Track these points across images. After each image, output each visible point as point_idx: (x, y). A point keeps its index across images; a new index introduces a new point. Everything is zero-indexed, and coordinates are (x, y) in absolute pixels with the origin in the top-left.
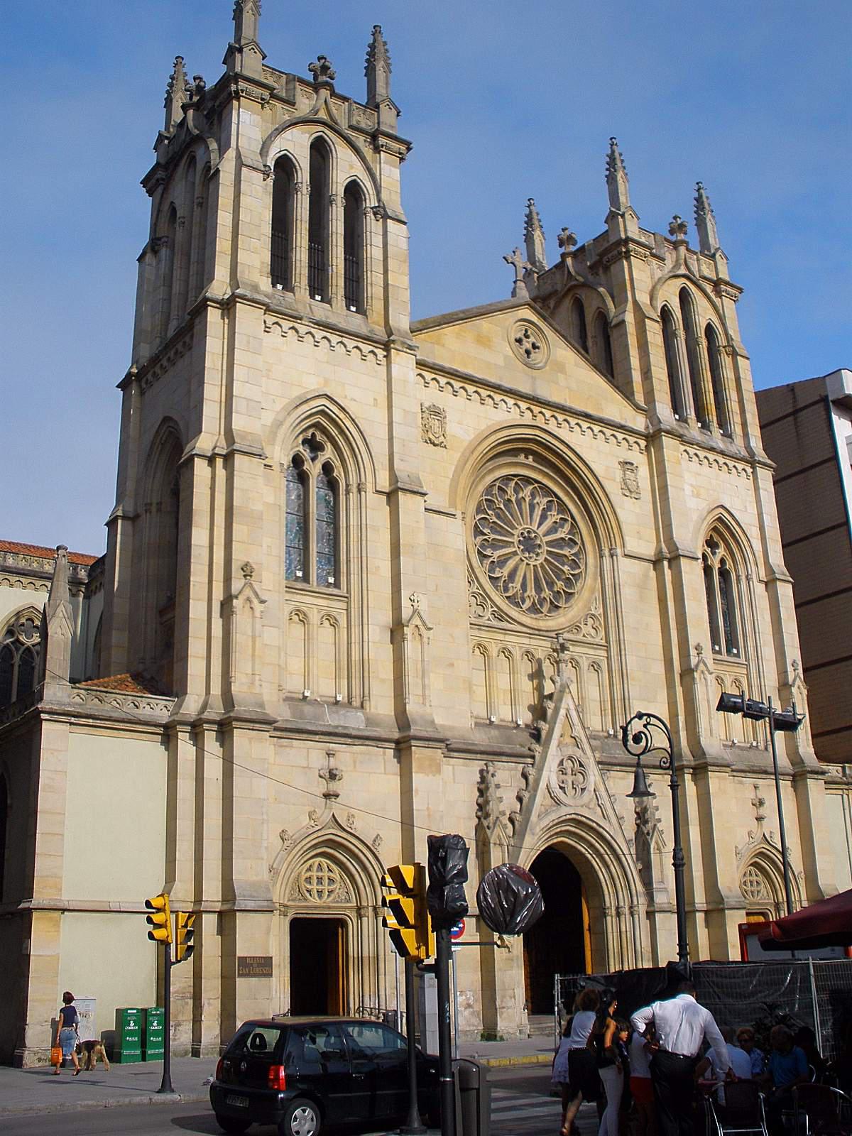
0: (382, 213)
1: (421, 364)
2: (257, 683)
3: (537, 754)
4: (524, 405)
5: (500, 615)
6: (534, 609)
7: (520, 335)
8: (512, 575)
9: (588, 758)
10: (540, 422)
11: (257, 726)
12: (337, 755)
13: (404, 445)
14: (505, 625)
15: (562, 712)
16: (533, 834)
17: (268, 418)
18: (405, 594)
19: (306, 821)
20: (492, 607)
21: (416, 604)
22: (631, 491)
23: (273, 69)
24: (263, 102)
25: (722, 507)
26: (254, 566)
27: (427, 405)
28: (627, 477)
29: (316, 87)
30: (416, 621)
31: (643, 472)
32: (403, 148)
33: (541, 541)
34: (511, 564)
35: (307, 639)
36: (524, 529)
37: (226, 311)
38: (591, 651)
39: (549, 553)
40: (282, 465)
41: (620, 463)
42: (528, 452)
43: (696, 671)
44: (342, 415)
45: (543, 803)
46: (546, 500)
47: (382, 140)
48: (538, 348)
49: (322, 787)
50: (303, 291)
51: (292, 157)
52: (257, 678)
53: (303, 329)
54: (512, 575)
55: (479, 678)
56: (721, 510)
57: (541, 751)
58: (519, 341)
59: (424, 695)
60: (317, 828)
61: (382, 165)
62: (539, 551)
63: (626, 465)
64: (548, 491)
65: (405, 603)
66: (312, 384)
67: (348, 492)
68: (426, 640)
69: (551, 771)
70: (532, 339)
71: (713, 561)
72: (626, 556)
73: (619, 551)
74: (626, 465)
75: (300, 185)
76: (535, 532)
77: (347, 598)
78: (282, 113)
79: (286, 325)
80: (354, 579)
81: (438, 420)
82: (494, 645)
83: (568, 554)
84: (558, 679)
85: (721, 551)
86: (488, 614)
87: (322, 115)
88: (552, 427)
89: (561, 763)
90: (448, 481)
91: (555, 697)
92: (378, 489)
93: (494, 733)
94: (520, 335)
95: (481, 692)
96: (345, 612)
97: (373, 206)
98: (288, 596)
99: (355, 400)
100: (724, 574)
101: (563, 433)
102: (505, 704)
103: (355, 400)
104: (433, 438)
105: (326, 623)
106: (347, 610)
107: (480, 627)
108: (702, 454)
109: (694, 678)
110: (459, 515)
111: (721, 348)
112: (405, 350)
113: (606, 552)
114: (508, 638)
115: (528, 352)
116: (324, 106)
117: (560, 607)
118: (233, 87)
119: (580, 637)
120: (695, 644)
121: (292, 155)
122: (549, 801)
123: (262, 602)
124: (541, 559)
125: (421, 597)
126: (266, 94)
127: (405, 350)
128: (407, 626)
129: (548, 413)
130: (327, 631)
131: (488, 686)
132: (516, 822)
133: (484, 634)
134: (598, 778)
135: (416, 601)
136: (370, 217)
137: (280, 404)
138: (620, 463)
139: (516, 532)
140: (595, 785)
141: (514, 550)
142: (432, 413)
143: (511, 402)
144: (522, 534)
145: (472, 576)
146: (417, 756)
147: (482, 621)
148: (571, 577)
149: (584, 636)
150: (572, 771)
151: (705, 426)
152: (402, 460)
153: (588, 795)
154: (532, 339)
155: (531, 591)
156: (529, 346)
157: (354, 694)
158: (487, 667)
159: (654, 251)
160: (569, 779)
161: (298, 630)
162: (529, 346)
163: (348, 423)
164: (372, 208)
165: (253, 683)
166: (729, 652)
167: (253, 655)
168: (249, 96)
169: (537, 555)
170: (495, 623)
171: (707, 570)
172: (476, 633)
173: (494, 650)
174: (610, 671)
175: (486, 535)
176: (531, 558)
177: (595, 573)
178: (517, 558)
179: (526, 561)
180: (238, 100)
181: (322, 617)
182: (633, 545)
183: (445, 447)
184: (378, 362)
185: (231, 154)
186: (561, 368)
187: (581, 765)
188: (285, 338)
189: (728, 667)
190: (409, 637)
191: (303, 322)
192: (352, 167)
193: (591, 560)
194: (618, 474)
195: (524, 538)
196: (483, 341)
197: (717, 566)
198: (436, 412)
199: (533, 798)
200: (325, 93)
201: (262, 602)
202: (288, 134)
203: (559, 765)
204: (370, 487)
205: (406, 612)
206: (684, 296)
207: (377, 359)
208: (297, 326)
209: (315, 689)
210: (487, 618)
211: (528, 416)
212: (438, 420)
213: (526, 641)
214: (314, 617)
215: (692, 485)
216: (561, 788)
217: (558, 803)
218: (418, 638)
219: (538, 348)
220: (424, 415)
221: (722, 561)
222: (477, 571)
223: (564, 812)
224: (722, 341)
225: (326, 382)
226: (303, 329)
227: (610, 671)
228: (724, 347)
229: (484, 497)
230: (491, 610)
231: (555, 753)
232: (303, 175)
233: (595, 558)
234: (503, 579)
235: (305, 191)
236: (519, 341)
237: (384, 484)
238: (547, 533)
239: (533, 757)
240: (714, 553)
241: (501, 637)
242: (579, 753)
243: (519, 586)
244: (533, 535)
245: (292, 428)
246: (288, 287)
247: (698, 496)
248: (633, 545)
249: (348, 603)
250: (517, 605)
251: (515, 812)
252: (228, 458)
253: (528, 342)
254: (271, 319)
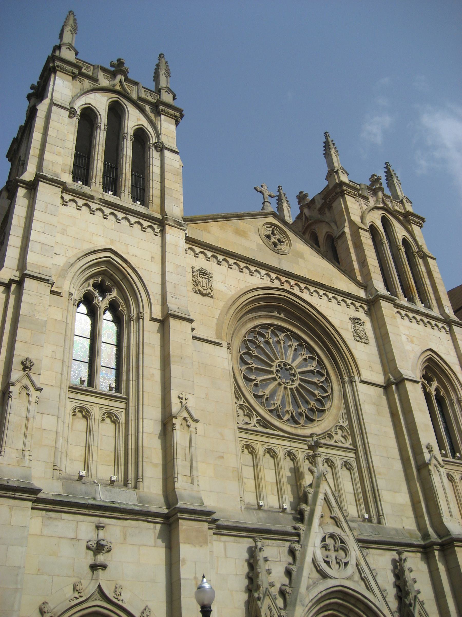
0: (161, 148)
1: (188, 240)
2: (27, 458)
3: (301, 532)
4: (273, 276)
5: (265, 423)
6: (294, 420)
7: (269, 232)
8: (273, 393)
9: (348, 536)
10: (286, 287)
11: (19, 495)
12: (107, 528)
13: (175, 288)
15: (321, 496)
16: (303, 605)
17: (61, 261)
18: (174, 394)
19: (69, 593)
20: (257, 417)
21: (184, 401)
22: (361, 338)
23: (84, 62)
24: (74, 77)
25: (431, 350)
26: (33, 361)
27: (197, 268)
28: (357, 328)
29: (113, 75)
30: (185, 414)
31: (368, 326)
32: (177, 114)
33: (295, 371)
35: (89, 431)
36: (281, 362)
37: (33, 190)
38: (343, 453)
39: (301, 380)
40: (71, 294)
41: (350, 319)
42: (280, 310)
43: (430, 464)
44: (124, 265)
45: (310, 576)
46: (296, 344)
47: (161, 107)
48: (283, 242)
49: (89, 558)
50: (97, 185)
51: (94, 108)
52: (27, 453)
53: (94, 206)
54: (273, 393)
55: (248, 472)
56: (430, 353)
57: (304, 529)
58: (268, 237)
59: (192, 476)
60: (81, 600)
61: (162, 122)
62: (294, 379)
63: (355, 320)
64: (298, 338)
65: (175, 400)
67: (129, 321)
68: (193, 430)
69: (315, 546)
70: (277, 236)
71: (430, 390)
72: (363, 382)
73: (357, 378)
74: (355, 320)
75: (99, 124)
76: (289, 365)
77: (126, 400)
78: (87, 84)
79: (81, 202)
80: (132, 384)
81: (206, 278)
82: (260, 446)
83: (317, 382)
84: (315, 469)
85: (435, 384)
86: (254, 421)
87: (118, 88)
88: (296, 291)
89: (324, 540)
90: (215, 320)
91: (314, 485)
92: (154, 316)
93: (261, 514)
94: (269, 232)
95: (250, 484)
96: (124, 410)
97: (154, 142)
98: (72, 395)
99: (136, 256)
100: (440, 401)
101: (305, 296)
102: (273, 494)
103: (136, 256)
104: (202, 289)
105: (108, 420)
106: (126, 409)
107: (247, 431)
108: (411, 315)
109: (429, 471)
110: (224, 344)
111: (415, 253)
112: (176, 226)
113: (347, 379)
114: (272, 441)
115: (275, 245)
116: (119, 84)
117: (315, 420)
118: (51, 65)
119: (332, 443)
120: (426, 444)
121: (95, 107)
122: (316, 575)
123: (40, 390)
124: (296, 384)
125: (188, 396)
126: (76, 71)
127: (176, 226)
128: (176, 418)
129: (293, 282)
130: (109, 426)
131: (257, 479)
132: (287, 595)
133: (251, 437)
134: (358, 553)
135: (184, 399)
136: (153, 150)
137: (73, 253)
138: (350, 319)
139: (274, 364)
140: (357, 560)
141: (273, 376)
142: (200, 273)
143: (263, 272)
144: (279, 366)
145: (239, 393)
146: (184, 527)
148: (321, 398)
149: (336, 442)
150: (334, 547)
151: (411, 300)
152: (174, 297)
153: (351, 569)
154: (277, 236)
155: (290, 407)
156: (276, 240)
157: (129, 477)
158: (255, 465)
159: (360, 192)
160: (333, 554)
161: (81, 424)
162: (276, 240)
163: (130, 271)
164: (154, 144)
165: (22, 457)
166: (454, 456)
167: (26, 433)
168: (63, 71)
169: (293, 381)
171: (427, 396)
172: (244, 435)
173: (260, 450)
174: (360, 469)
175: (250, 364)
176: (288, 383)
177: (340, 396)
178: (276, 383)
179: (283, 385)
180: (55, 73)
181: (104, 414)
182: (366, 375)
183: (212, 297)
184: (155, 233)
185: (46, 102)
186: (300, 255)
187: (342, 542)
188: (80, 211)
189: (455, 467)
190: (178, 426)
191: (95, 201)
192: (139, 120)
193: (336, 387)
194: (350, 326)
195: (281, 369)
197: (434, 393)
198: (203, 273)
199: (301, 569)
200: (120, 77)
201: (40, 390)
203: (322, 542)
204: (146, 316)
205: (175, 407)
206: (384, 220)
207: (154, 232)
208: (90, 203)
209: (94, 472)
210: (253, 424)
212: (206, 278)
213: (287, 443)
214: (96, 413)
215: (406, 335)
216: (325, 561)
217: (324, 576)
218: (186, 428)
219: (283, 242)
220: (194, 274)
221: (437, 390)
222: (243, 389)
223: (330, 583)
224: (415, 249)
226: (94, 206)
227: (360, 469)
228: (416, 253)
229: (247, 338)
230: (256, 419)
231: (317, 531)
232: (103, 119)
233: (339, 385)
234: (266, 397)
235: (102, 128)
236: (268, 237)
237: (157, 313)
238: (299, 366)
239: (298, 535)
240: (431, 385)
241: (266, 440)
242: (337, 531)
243: (279, 403)
244: (288, 367)
245: (81, 270)
246: (87, 182)
247: (412, 342)
248: (366, 375)
249: (126, 404)
250: (279, 417)
251: (284, 585)
252: (20, 283)
253: (275, 238)
254: (67, 197)
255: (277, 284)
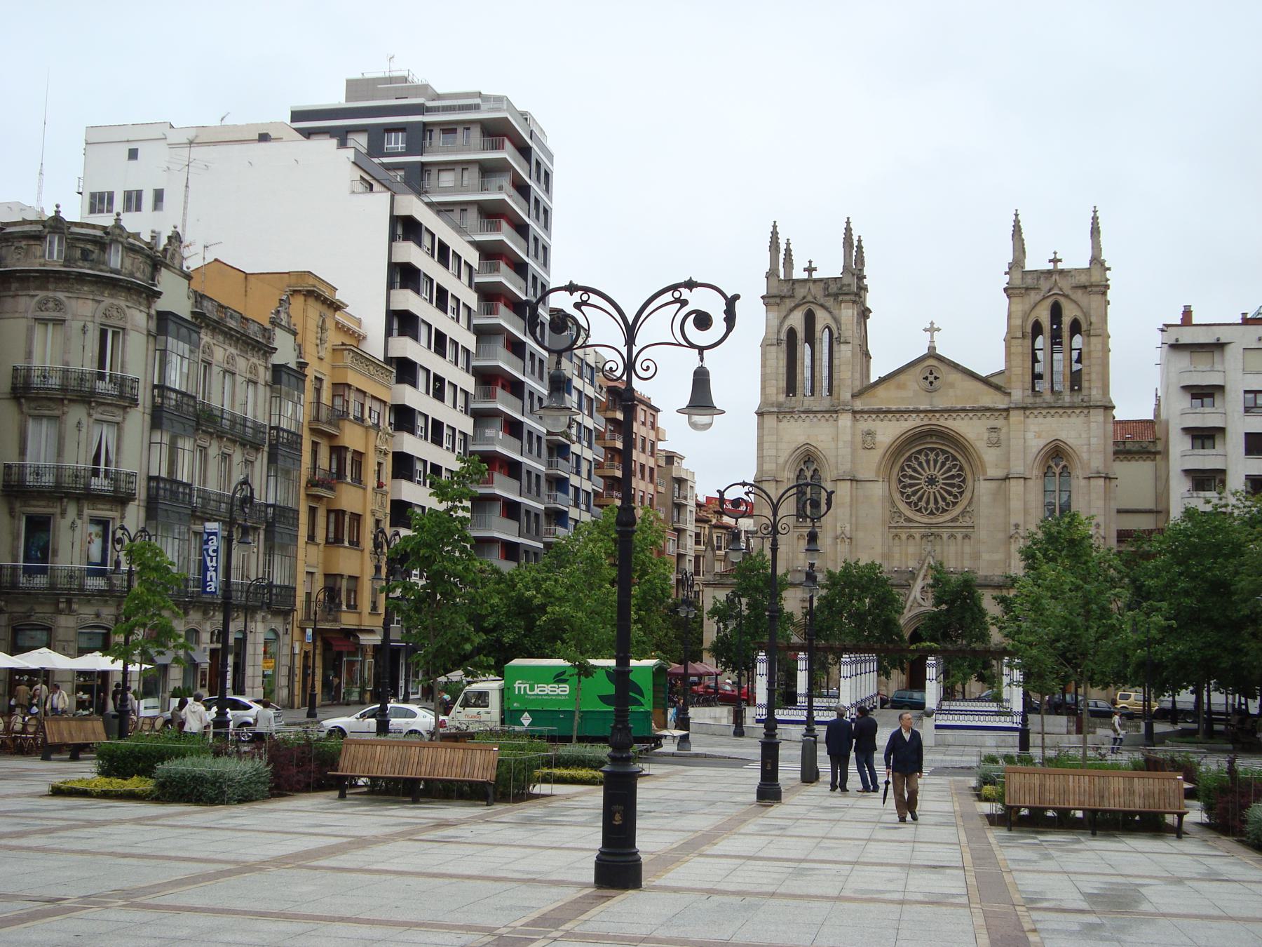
5: (908, 520)
14: (911, 525)
17: (781, 460)
18: (839, 525)
34: (920, 493)
42: (931, 436)
53: (796, 416)
58: (926, 378)
65: (839, 528)
66: (802, 439)
79: (788, 416)
87: (810, 298)
110: (881, 479)
119: (958, 524)
124: (938, 488)
137: (789, 451)
147: (900, 524)
170: (905, 524)
186: (952, 385)
193: (969, 482)
196: (900, 387)
202: (792, 316)
211: (926, 419)
225: (808, 437)
247: (1039, 437)
255: (926, 422)
